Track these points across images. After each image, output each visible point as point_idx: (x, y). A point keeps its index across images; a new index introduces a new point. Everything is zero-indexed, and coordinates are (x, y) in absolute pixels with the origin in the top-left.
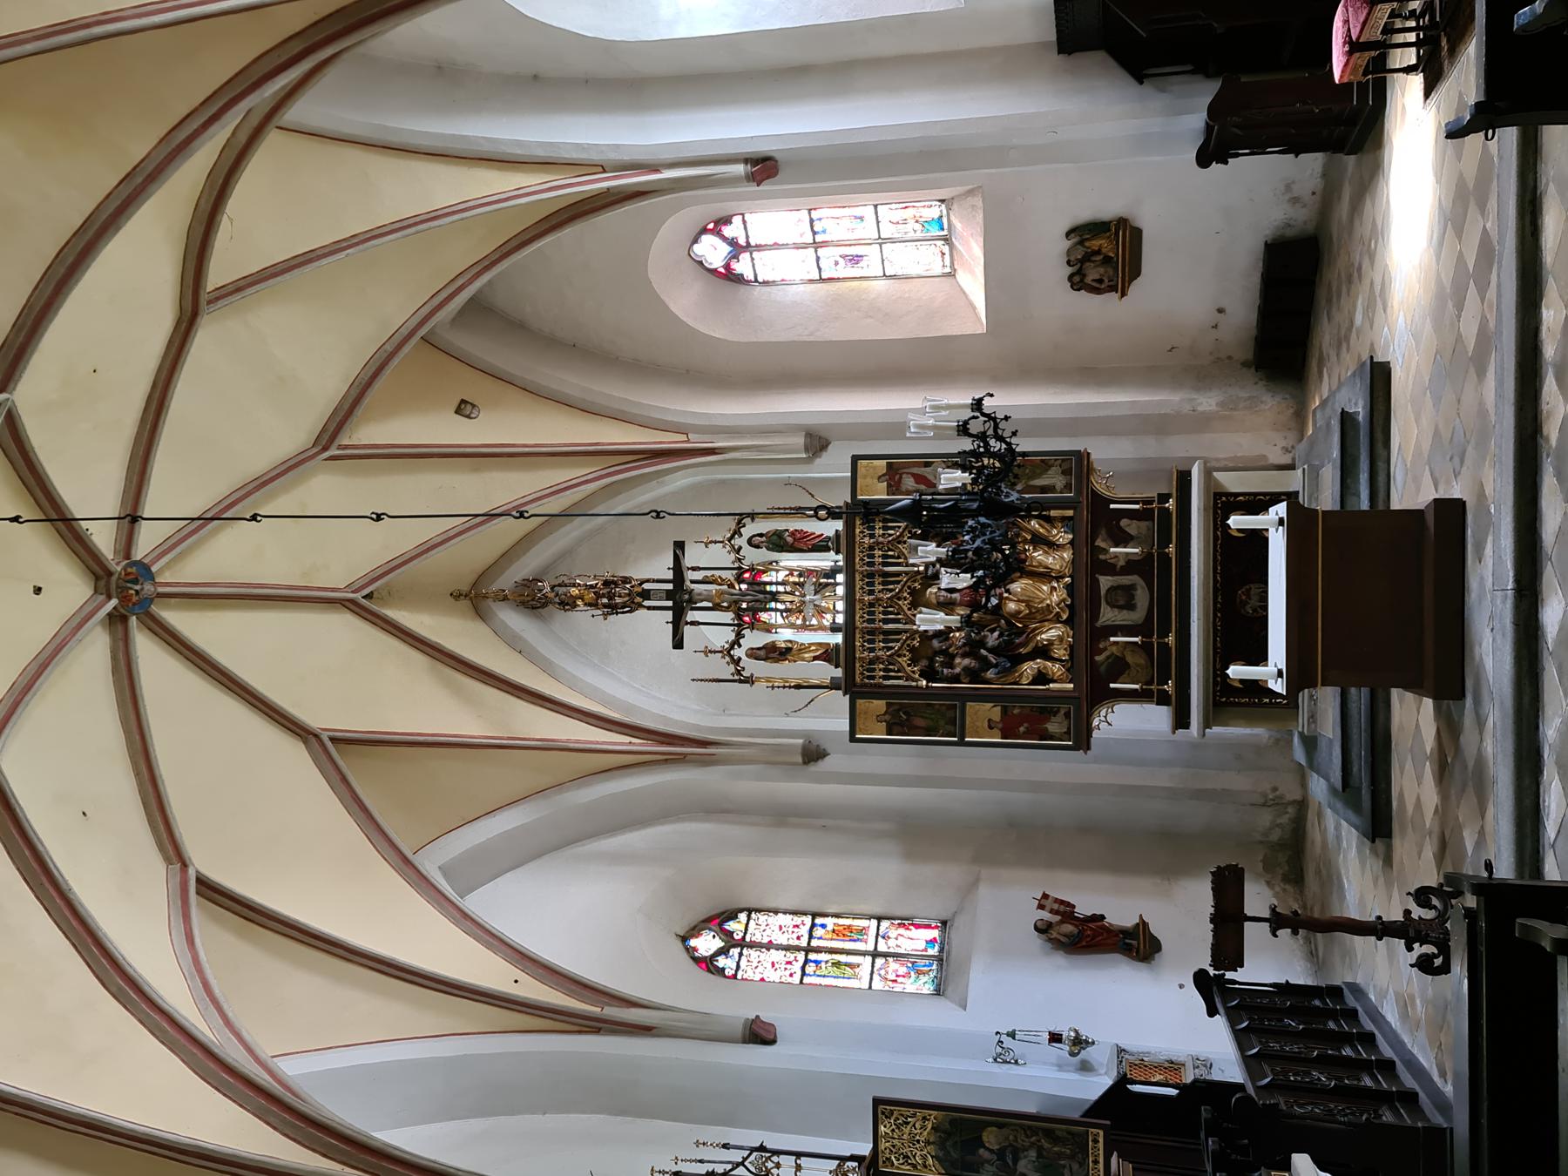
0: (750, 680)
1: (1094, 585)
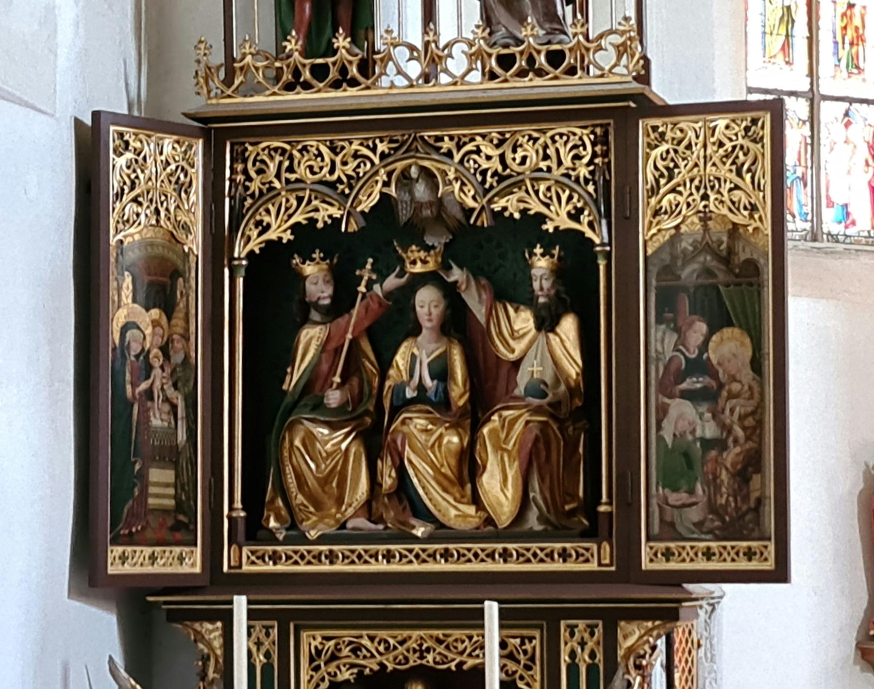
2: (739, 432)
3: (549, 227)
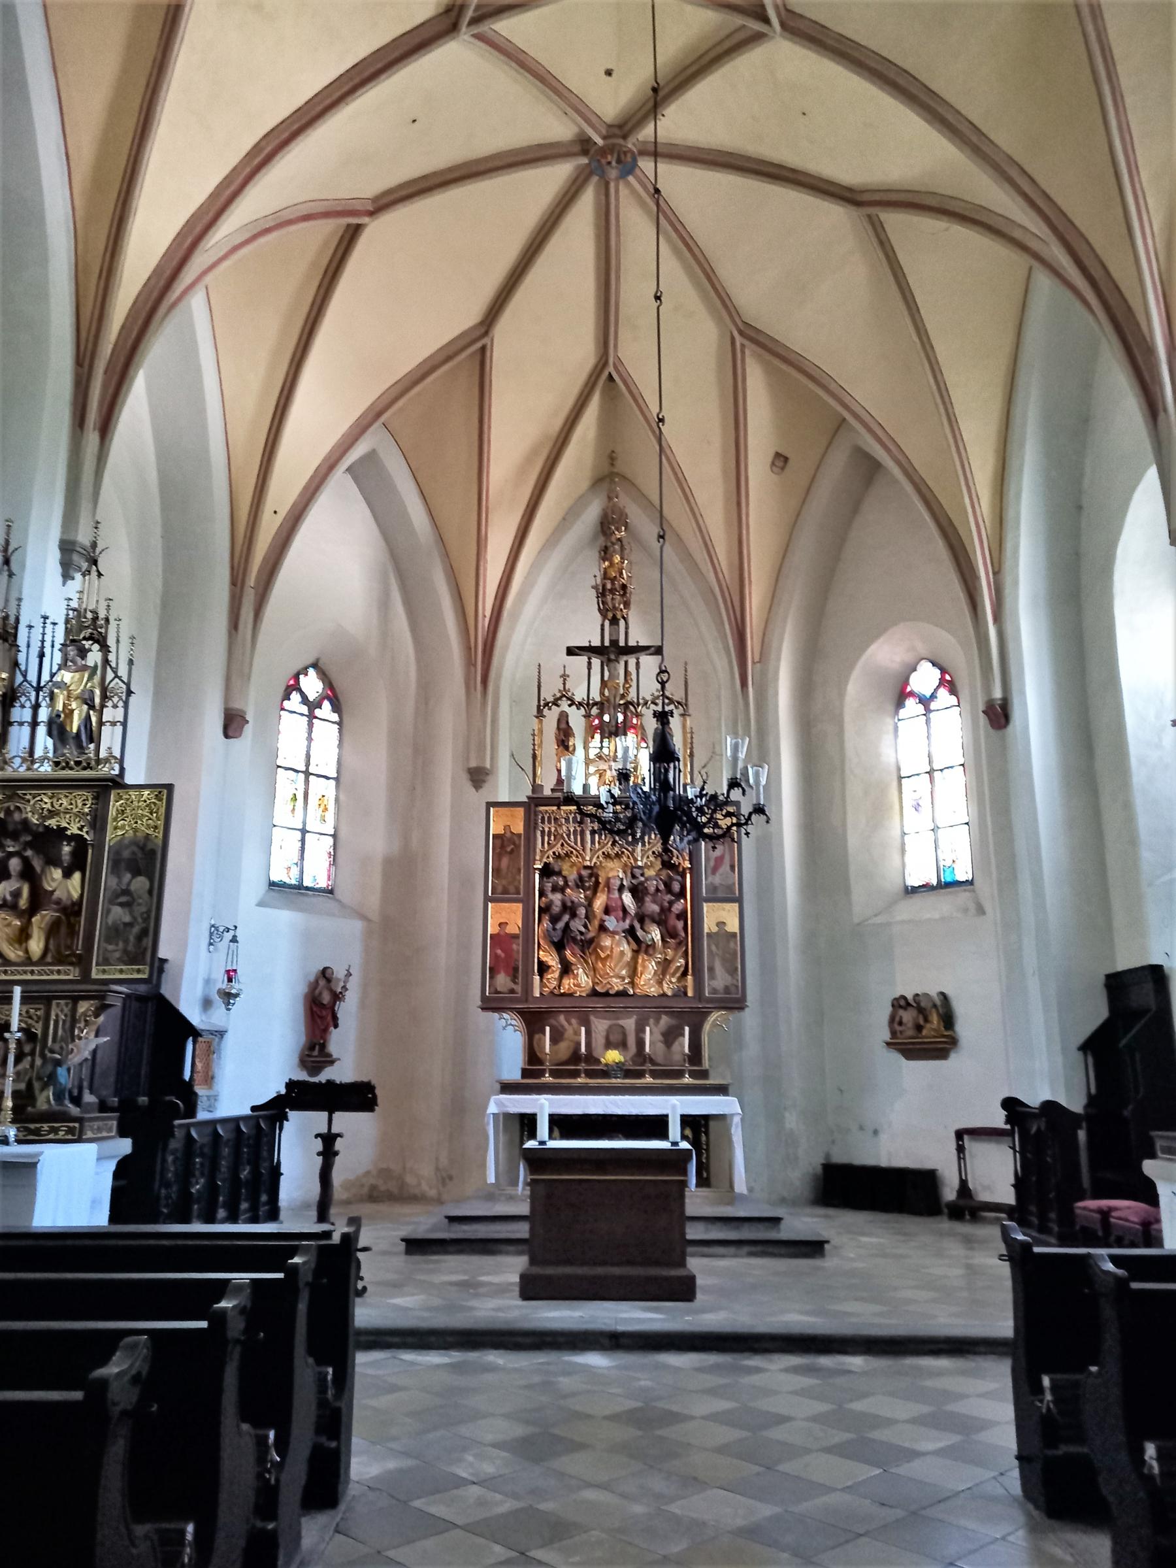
0: (540, 711)
1: (626, 1012)
2: (140, 920)
3: (69, 833)
